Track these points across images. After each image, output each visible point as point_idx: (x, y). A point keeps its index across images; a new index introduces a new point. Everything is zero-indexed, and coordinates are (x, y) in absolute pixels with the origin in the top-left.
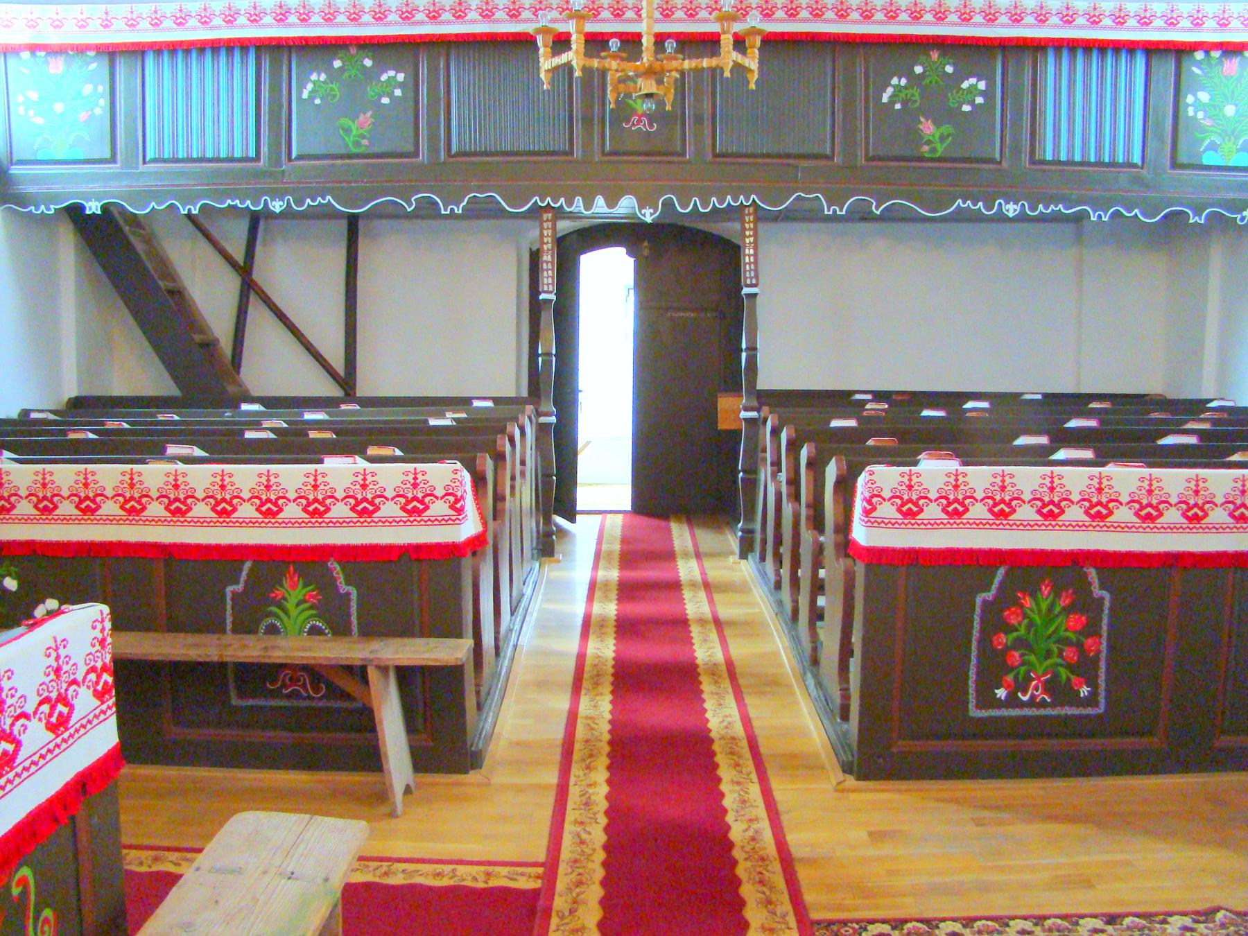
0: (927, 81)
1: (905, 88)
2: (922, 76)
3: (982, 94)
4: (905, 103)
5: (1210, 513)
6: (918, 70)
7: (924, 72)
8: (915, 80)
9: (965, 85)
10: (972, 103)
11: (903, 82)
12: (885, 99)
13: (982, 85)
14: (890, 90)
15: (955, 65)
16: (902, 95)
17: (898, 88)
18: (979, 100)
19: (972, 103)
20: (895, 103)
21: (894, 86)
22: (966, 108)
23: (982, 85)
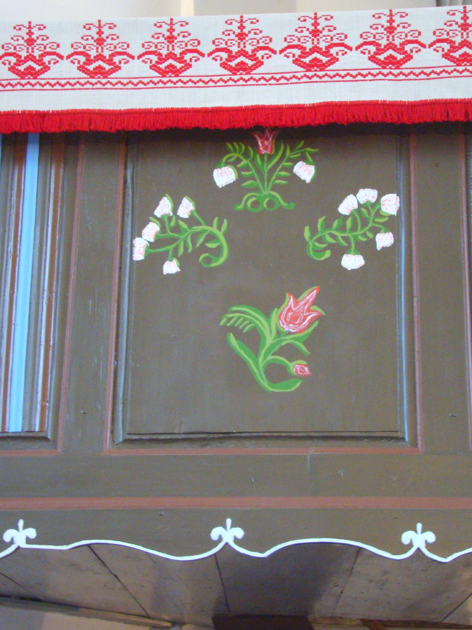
0: (248, 201)
1: (191, 221)
2: (234, 189)
3: (391, 224)
6: (224, 176)
7: (240, 179)
8: (212, 203)
9: (347, 206)
10: (366, 249)
11: (187, 208)
13: (391, 204)
14: (151, 231)
15: (316, 160)
16: (184, 243)
18: (384, 240)
20: (164, 258)
21: (161, 221)
22: (352, 262)
23: (391, 204)
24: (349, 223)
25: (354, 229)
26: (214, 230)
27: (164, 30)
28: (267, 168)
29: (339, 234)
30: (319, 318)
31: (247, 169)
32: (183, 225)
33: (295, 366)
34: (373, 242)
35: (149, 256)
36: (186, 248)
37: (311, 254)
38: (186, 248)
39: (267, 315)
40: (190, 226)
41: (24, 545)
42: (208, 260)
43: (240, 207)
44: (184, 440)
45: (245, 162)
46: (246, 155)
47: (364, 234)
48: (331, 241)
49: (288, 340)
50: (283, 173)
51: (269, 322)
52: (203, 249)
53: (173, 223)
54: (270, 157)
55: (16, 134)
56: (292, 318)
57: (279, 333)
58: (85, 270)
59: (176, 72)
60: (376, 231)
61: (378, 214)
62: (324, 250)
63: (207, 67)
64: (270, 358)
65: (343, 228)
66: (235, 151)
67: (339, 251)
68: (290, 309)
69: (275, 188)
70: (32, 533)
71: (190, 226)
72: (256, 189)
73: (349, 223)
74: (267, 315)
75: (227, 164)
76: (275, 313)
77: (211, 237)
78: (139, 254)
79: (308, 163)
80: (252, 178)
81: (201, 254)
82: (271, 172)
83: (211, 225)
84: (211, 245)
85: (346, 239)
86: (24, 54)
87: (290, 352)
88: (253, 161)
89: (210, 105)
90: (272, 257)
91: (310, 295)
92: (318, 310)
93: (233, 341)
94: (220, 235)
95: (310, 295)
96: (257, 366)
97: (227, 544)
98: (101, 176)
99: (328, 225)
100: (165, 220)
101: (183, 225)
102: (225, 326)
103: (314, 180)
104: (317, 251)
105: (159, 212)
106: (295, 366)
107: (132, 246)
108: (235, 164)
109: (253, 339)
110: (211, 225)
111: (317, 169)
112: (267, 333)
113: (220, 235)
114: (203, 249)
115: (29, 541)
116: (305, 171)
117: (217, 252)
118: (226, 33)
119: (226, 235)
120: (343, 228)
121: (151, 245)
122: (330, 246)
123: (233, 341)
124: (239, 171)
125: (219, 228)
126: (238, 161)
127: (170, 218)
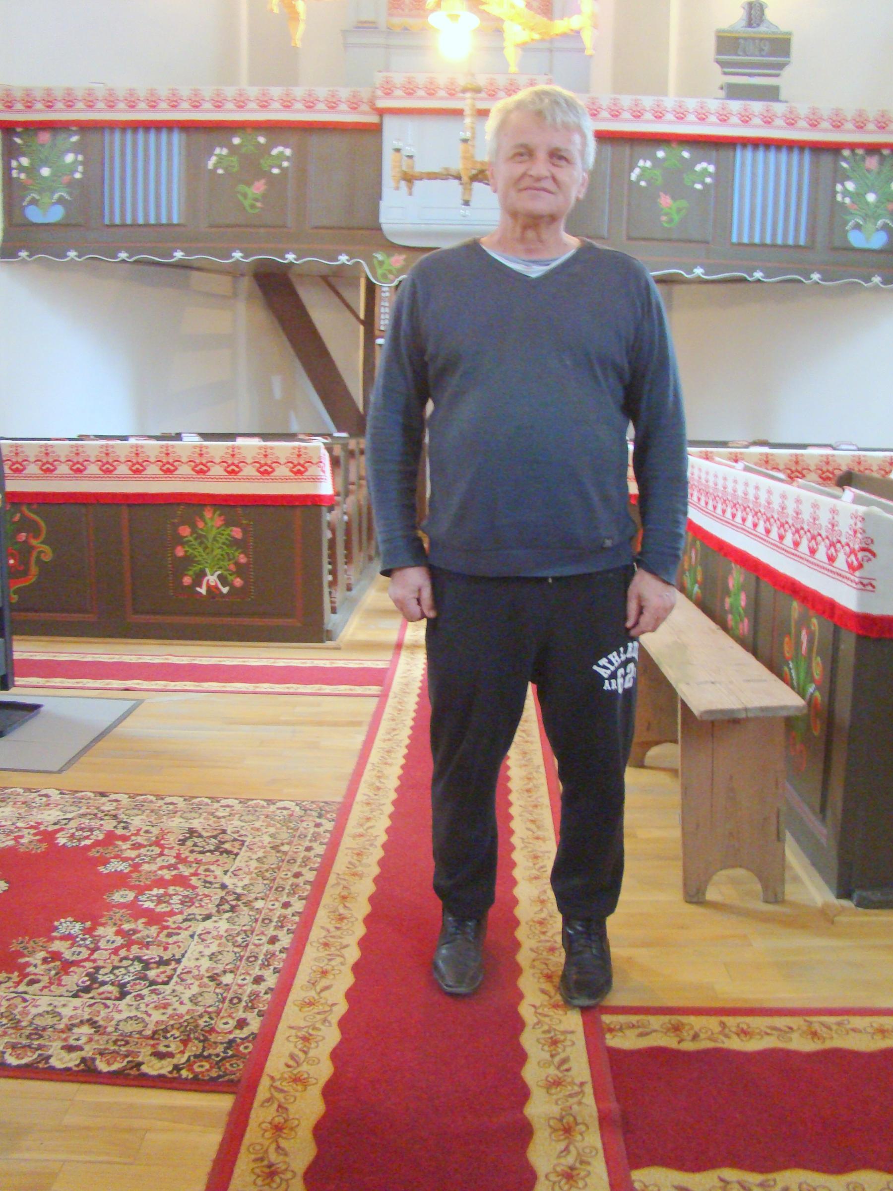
3: (287, 159)
4: (225, 169)
5: (277, 469)
6: (236, 141)
8: (233, 149)
10: (280, 167)
13: (288, 152)
14: (214, 159)
17: (220, 157)
18: (285, 164)
21: (217, 155)
22: (276, 171)
56: (258, 188)
87: (256, 200)
106: (259, 204)
109: (245, 196)
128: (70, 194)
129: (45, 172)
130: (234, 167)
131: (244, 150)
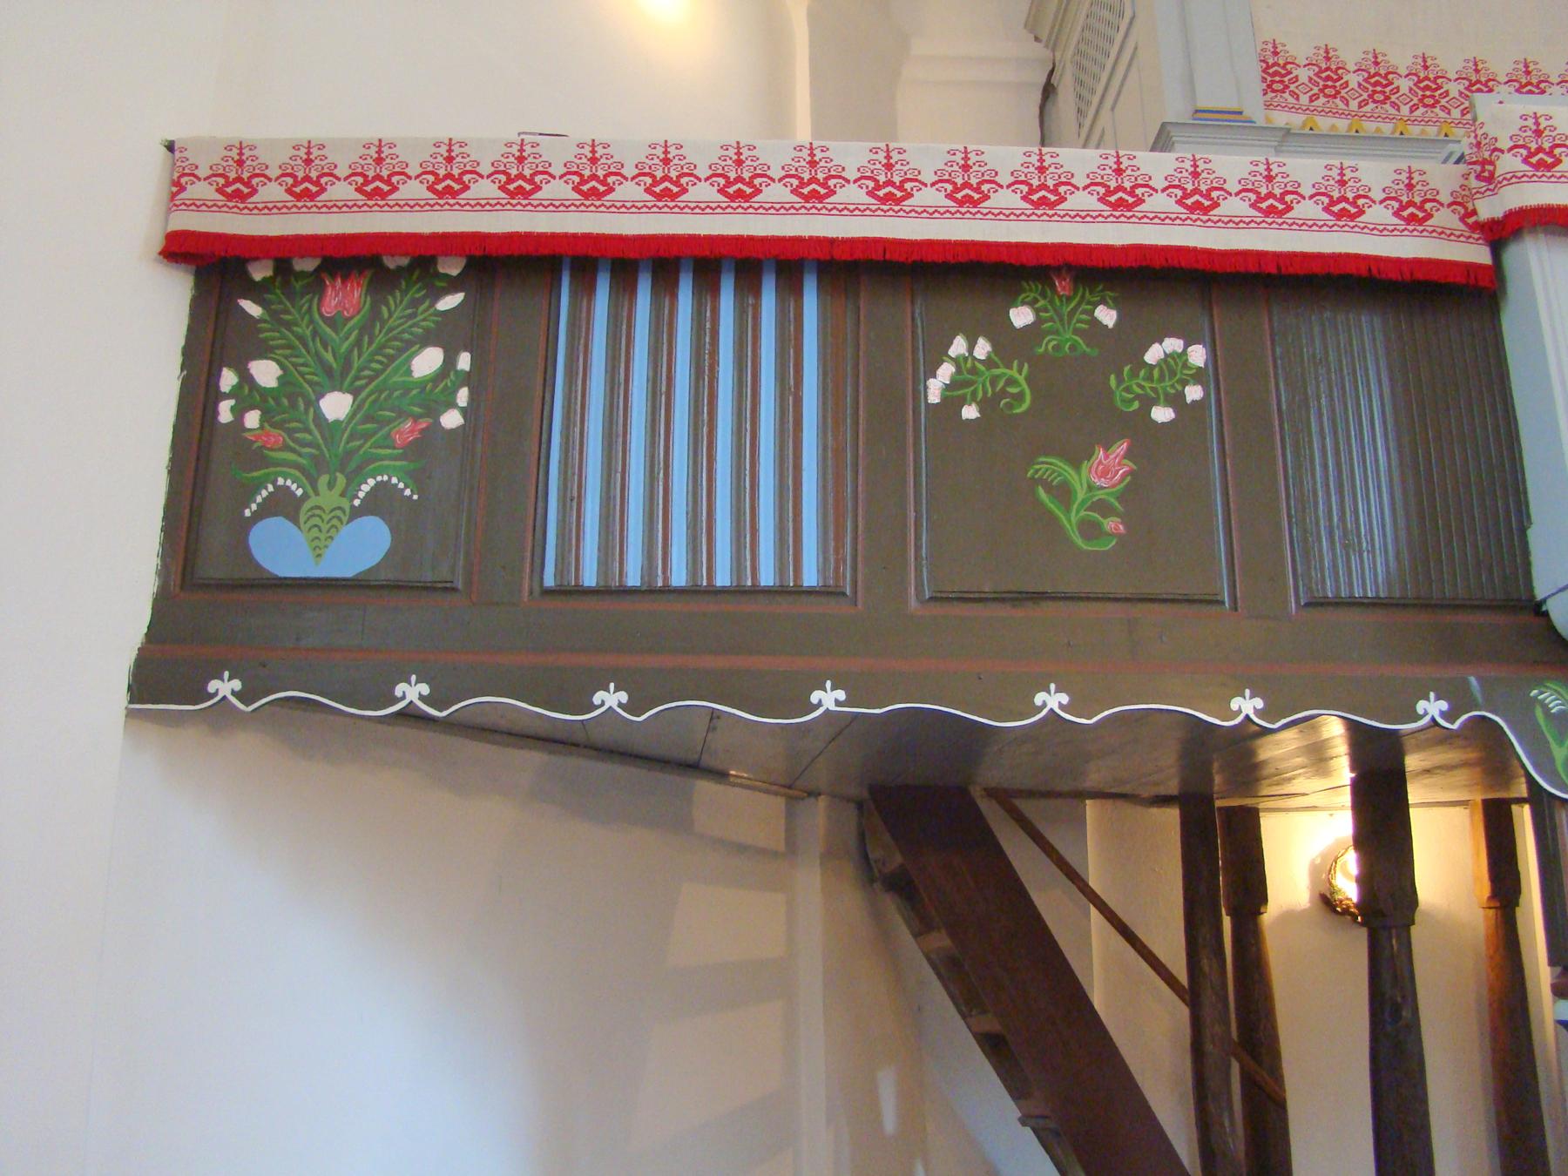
0: (1047, 345)
1: (989, 363)
2: (1033, 331)
3: (1198, 376)
6: (1021, 316)
7: (1039, 322)
8: (1010, 344)
9: (1153, 354)
11: (983, 349)
12: (935, 390)
13: (1198, 355)
14: (946, 372)
15: (1116, 304)
16: (982, 387)
18: (1194, 393)
19: (1176, 401)
20: (962, 402)
21: (955, 361)
23: (1198, 355)
24: (1156, 373)
25: (1162, 378)
26: (1014, 373)
27: (959, 158)
28: (1066, 310)
29: (1147, 385)
30: (1130, 472)
31: (1046, 310)
32: (981, 367)
33: (1110, 524)
34: (1182, 395)
35: (944, 399)
36: (985, 392)
37: (1119, 404)
38: (985, 392)
39: (1077, 468)
40: (989, 368)
41: (833, 708)
42: (1010, 406)
43: (1041, 350)
44: (994, 599)
45: (1041, 303)
46: (1043, 295)
47: (1173, 386)
48: (1139, 391)
49: (1100, 495)
50: (1084, 317)
51: (1079, 473)
52: (1003, 393)
53: (969, 365)
54: (1069, 299)
55: (586, 257)
56: (1106, 469)
57: (1090, 488)
58: (872, 413)
59: (975, 203)
60: (1184, 383)
61: (1186, 365)
62: (1131, 401)
63: (852, 194)
64: (1083, 513)
65: (1150, 378)
66: (1032, 290)
67: (1148, 403)
68: (1100, 463)
69: (1076, 332)
70: (841, 695)
71: (989, 368)
72: (1056, 332)
73: (1156, 373)
74: (1077, 468)
75: (1023, 303)
76: (1085, 466)
77: (1011, 382)
78: (934, 397)
79: (1109, 307)
80: (1051, 319)
81: (1033, 401)
82: (1072, 313)
83: (1010, 368)
84: (1013, 390)
85: (1154, 390)
86: (806, 176)
87: (1103, 508)
88: (1051, 302)
89: (1013, 239)
90: (1077, 405)
91: (1121, 447)
92: (1129, 464)
93: (1042, 493)
94: (1021, 379)
95: (1121, 447)
96: (1070, 521)
97: (1052, 710)
98: (905, 313)
99: (1134, 374)
100: (956, 363)
101: (981, 367)
102: (1032, 478)
103: (1117, 324)
104: (1124, 401)
105: (952, 352)
106: (1110, 524)
107: (926, 388)
108: (1032, 304)
109: (1063, 493)
110: (1010, 368)
111: (1119, 316)
112: (1078, 486)
113: (1021, 379)
114: (1003, 393)
115: (838, 703)
116: (1107, 316)
117: (1019, 397)
118: (1025, 165)
119: (1028, 380)
120: (1150, 378)
121: (947, 387)
122: (1138, 397)
123: (1042, 493)
124: (1037, 311)
125: (1020, 372)
126: (1035, 301)
127: (966, 359)
128: (417, 478)
129: (336, 406)
130: (1019, 397)
131: (1047, 345)
